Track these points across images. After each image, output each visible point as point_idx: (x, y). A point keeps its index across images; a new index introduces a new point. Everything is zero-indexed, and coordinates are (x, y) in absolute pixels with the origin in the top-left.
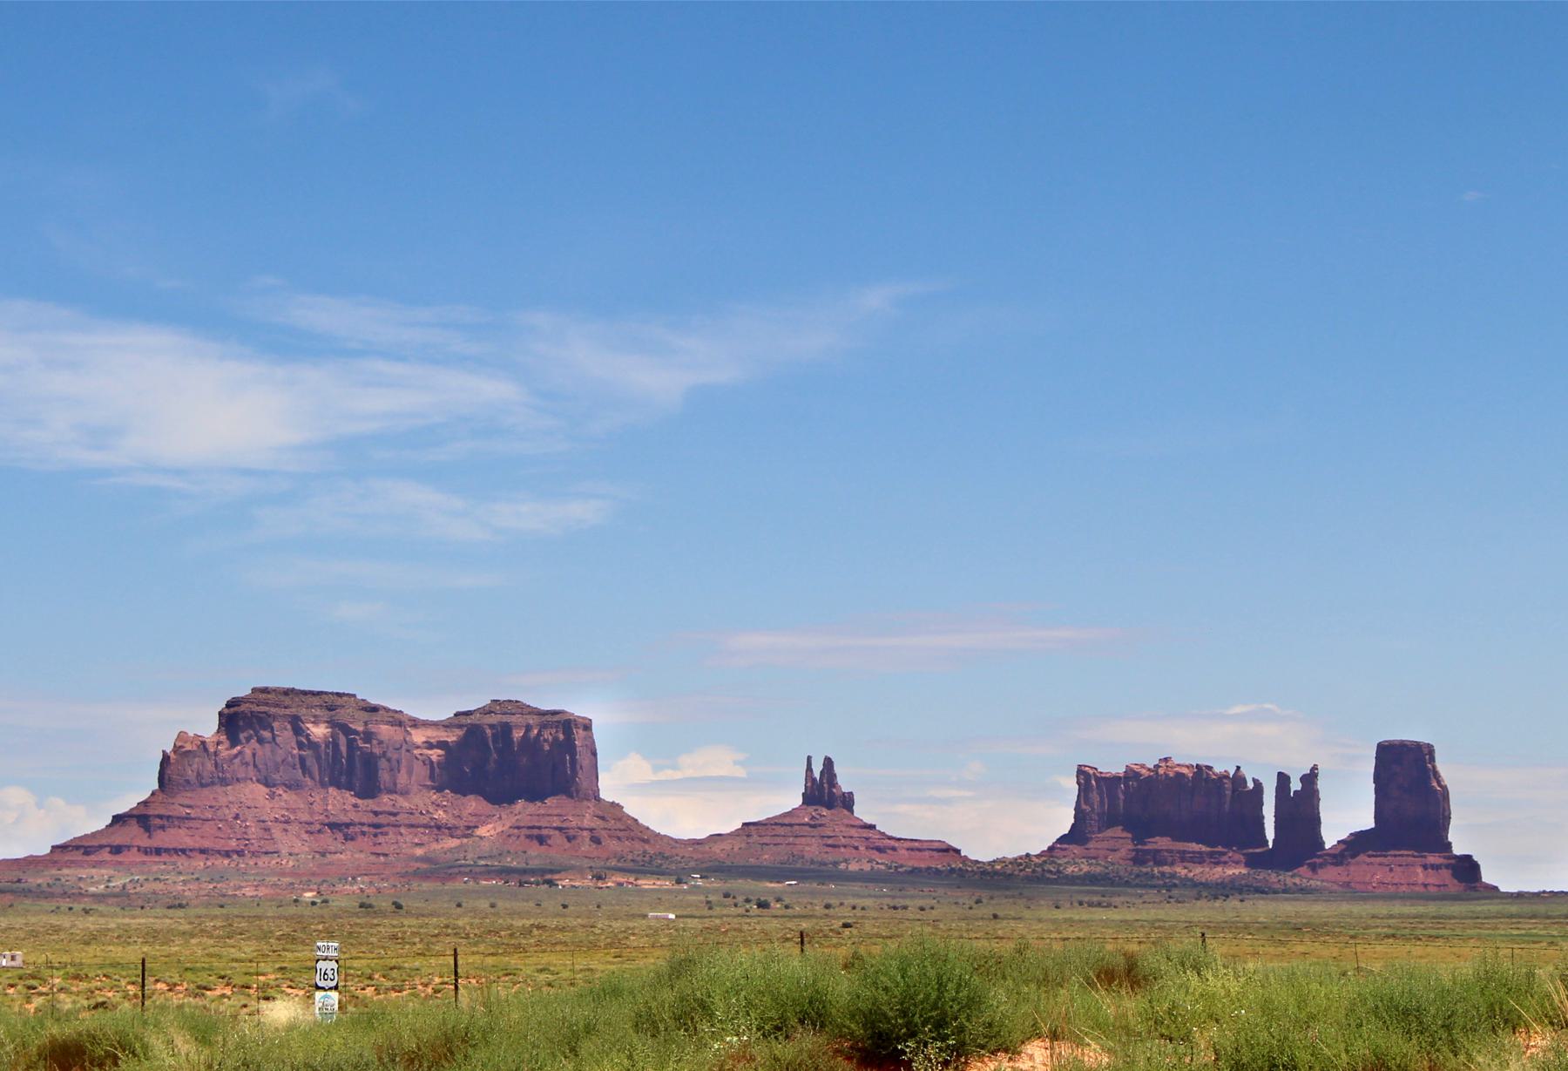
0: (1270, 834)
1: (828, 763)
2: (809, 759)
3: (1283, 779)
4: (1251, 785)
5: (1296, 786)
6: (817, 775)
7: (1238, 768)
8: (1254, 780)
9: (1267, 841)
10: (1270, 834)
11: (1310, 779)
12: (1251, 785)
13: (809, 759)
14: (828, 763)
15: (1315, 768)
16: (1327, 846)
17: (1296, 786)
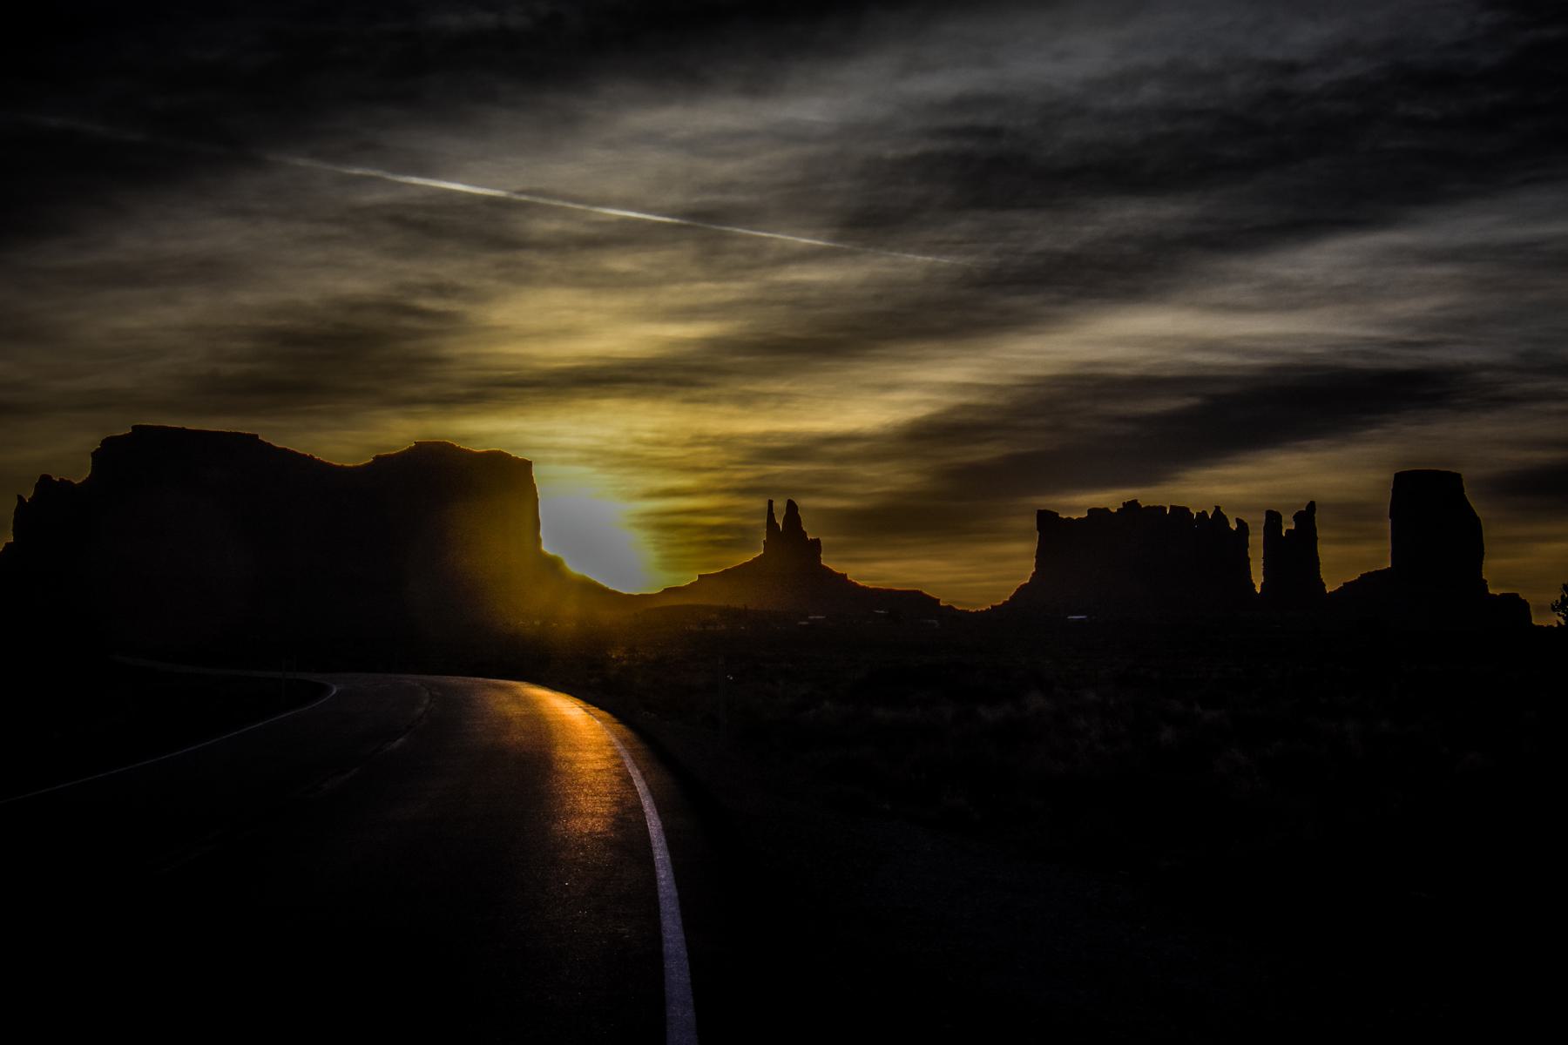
0: (1258, 580)
1: (792, 507)
2: (771, 502)
3: (1273, 518)
4: (1234, 526)
5: (1288, 525)
6: (780, 521)
7: (1218, 508)
8: (1239, 521)
9: (1254, 586)
10: (1258, 580)
11: (1306, 517)
12: (1234, 526)
13: (771, 502)
14: (792, 507)
15: (1312, 506)
16: (1328, 592)
17: (1288, 525)
